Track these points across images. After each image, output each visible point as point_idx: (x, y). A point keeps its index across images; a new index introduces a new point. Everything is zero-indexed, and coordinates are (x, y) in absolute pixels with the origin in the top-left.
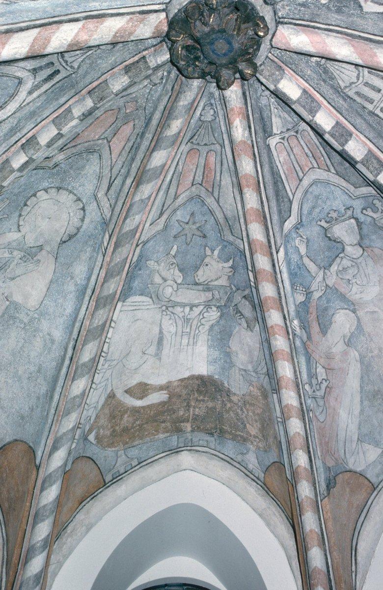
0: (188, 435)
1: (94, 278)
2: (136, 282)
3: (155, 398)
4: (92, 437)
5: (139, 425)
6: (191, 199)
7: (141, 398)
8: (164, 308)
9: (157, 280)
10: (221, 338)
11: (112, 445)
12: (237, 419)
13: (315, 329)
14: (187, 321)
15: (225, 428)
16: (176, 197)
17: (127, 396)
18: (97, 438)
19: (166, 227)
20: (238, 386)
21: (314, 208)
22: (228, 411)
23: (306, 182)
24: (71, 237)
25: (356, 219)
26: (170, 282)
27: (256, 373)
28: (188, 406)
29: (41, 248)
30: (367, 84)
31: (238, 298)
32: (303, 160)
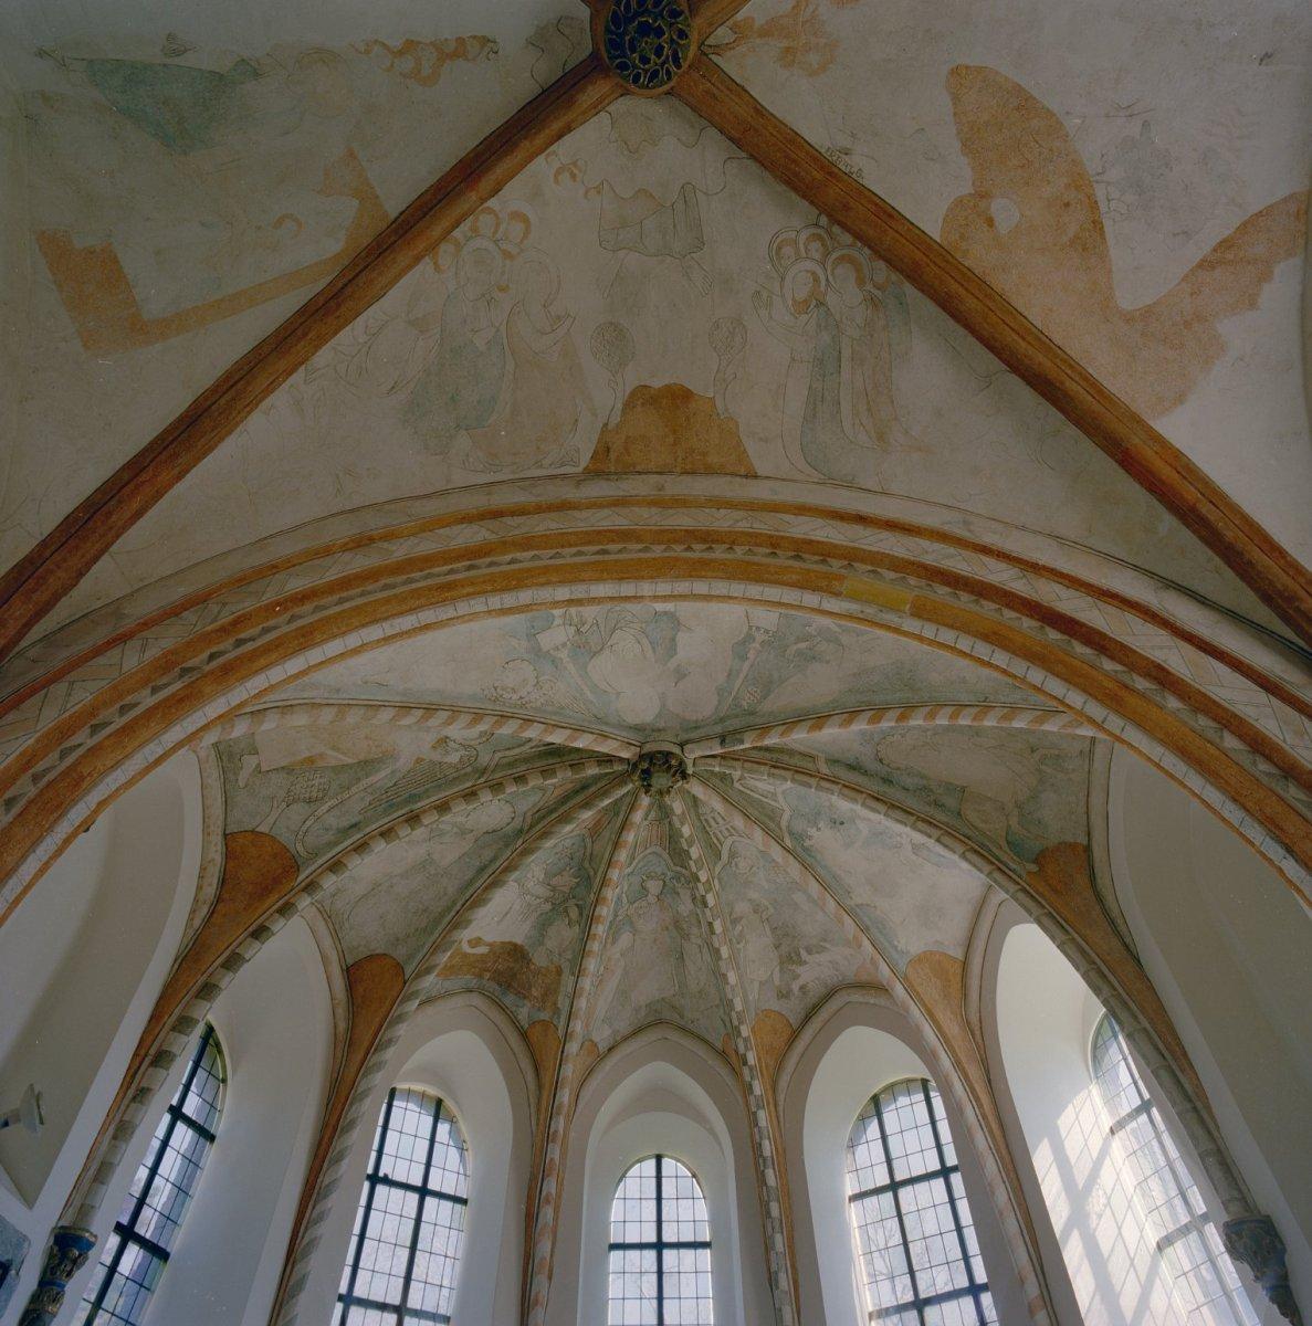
1: (498, 864)
3: (483, 950)
9: (529, 876)
10: (543, 926)
13: (609, 941)
20: (539, 959)
24: (494, 831)
27: (560, 955)
28: (495, 962)
30: (714, 818)
32: (655, 837)
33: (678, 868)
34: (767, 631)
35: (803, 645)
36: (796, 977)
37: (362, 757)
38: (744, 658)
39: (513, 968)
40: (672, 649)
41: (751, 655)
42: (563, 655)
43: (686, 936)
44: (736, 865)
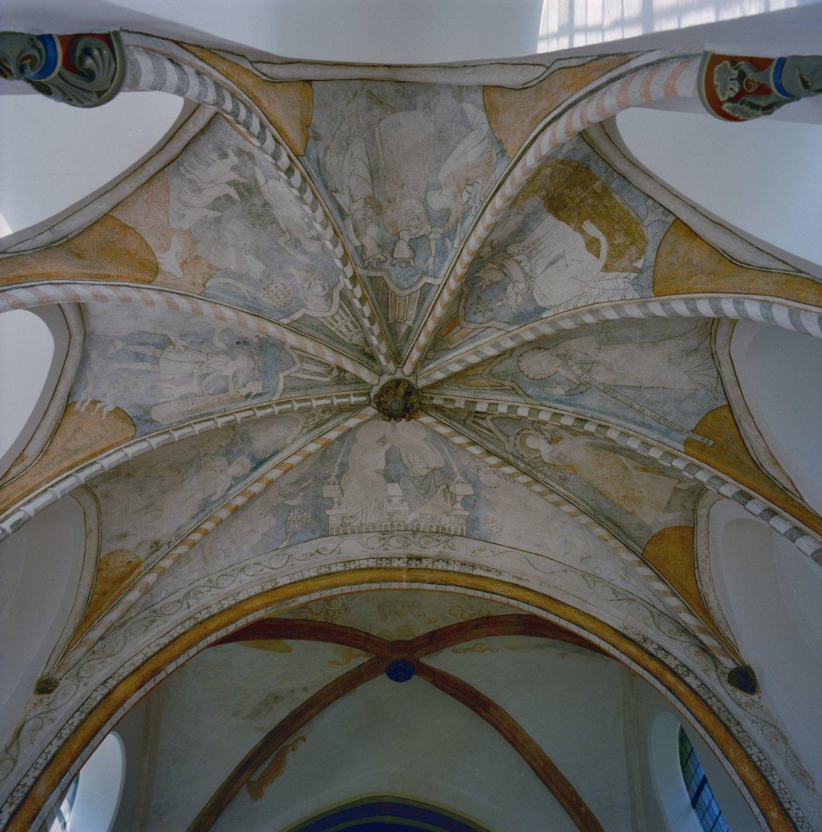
0: (603, 179)
2: (531, 309)
3: (591, 229)
4: (639, 264)
5: (619, 225)
6: (469, 322)
7: (598, 240)
8: (532, 279)
9: (520, 299)
10: (522, 231)
11: (643, 237)
12: (554, 178)
13: (452, 219)
14: (529, 257)
15: (572, 171)
16: (475, 329)
17: (601, 256)
18: (639, 258)
19: (492, 319)
20: (535, 202)
21: (412, 276)
22: (558, 184)
23: (407, 292)
24: (540, 349)
25: (392, 256)
26: (517, 290)
28: (582, 201)
29: (558, 356)
31: (486, 257)
33: (379, 274)
34: (329, 484)
35: (304, 485)
36: (234, 168)
37: (612, 454)
38: (341, 465)
39: (567, 187)
40: (388, 455)
41: (336, 468)
42: (459, 478)
43: (370, 201)
44: (324, 288)
